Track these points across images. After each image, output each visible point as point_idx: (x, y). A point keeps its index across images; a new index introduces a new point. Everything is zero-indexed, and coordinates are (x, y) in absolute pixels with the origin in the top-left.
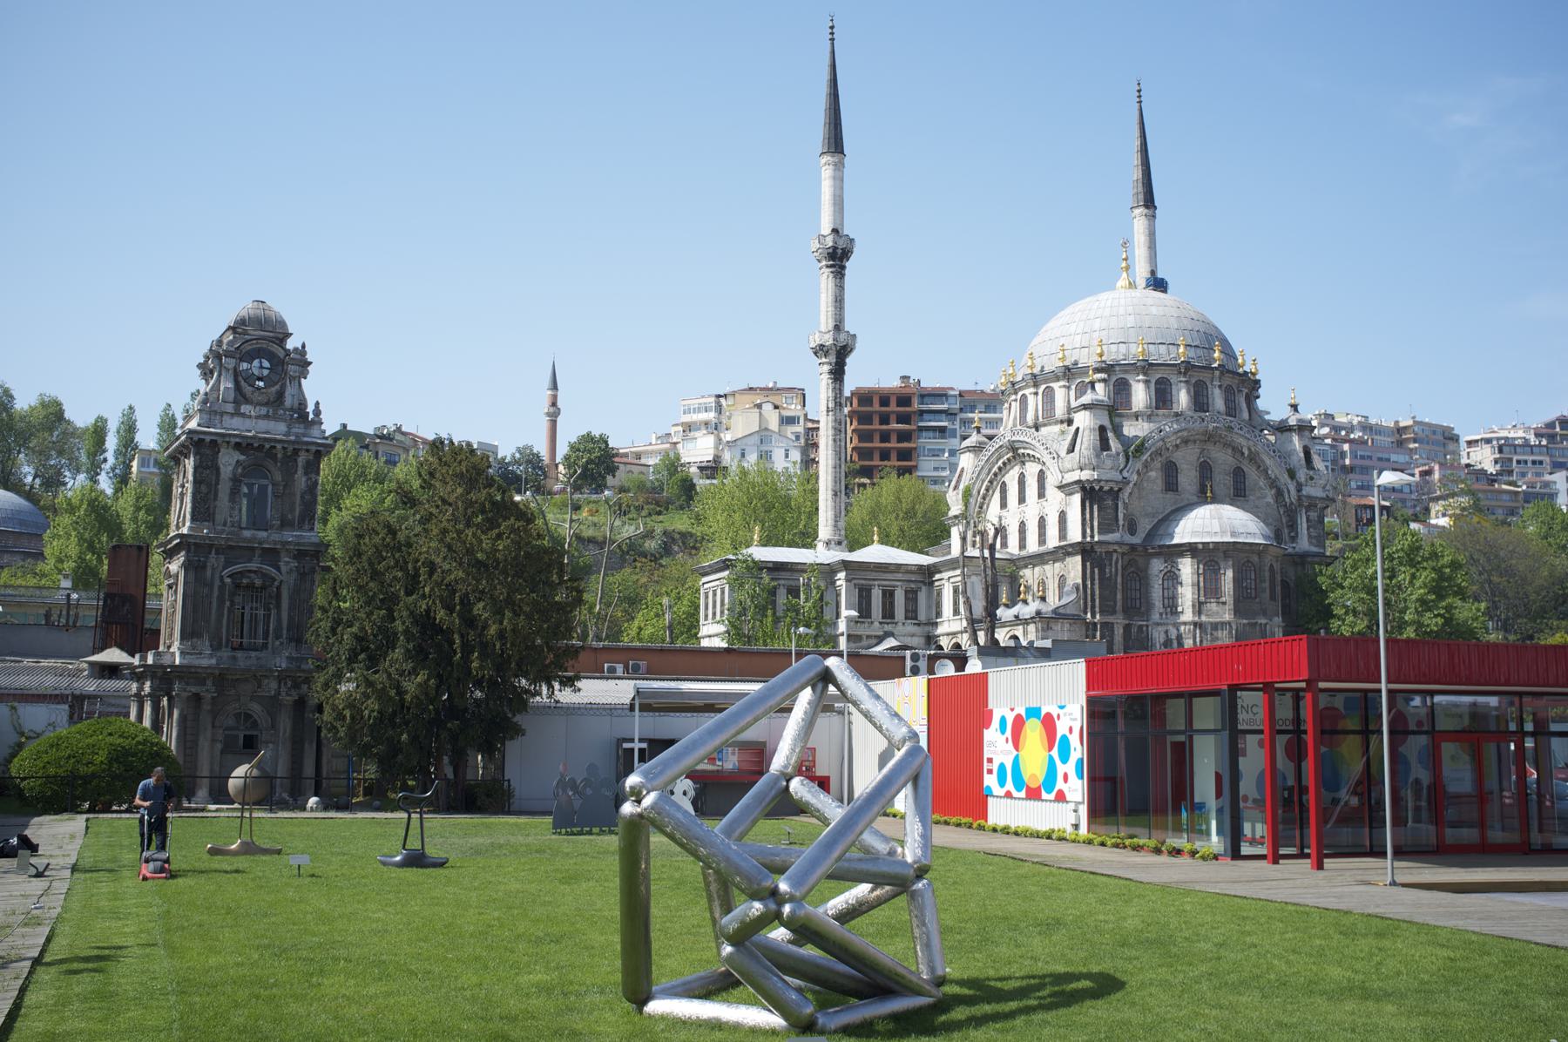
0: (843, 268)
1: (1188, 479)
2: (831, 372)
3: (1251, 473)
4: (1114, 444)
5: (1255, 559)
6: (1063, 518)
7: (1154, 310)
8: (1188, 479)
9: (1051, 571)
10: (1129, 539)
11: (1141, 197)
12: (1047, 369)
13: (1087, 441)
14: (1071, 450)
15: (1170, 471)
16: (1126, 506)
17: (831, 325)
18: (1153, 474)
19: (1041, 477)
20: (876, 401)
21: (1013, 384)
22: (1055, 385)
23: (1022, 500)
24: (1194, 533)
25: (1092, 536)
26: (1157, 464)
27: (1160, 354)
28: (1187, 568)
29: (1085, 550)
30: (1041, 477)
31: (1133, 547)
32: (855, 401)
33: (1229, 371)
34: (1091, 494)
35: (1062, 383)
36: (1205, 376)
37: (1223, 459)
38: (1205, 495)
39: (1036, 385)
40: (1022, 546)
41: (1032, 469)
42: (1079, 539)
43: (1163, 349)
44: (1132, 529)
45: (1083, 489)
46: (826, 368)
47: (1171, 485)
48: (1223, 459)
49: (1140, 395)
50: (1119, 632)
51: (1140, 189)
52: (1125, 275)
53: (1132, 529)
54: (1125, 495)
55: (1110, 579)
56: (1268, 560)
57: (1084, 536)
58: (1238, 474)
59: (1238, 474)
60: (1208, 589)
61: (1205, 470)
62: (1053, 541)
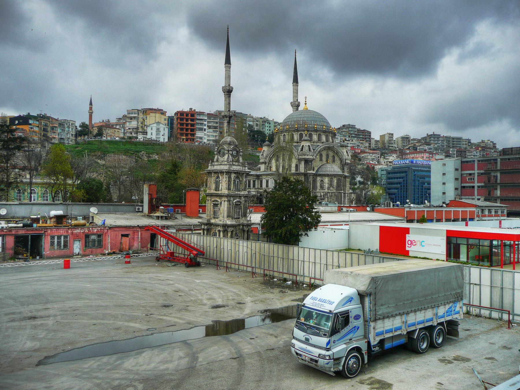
15: (321, 156)
20: (185, 115)
32: (179, 114)
59: (334, 157)
61: (328, 156)
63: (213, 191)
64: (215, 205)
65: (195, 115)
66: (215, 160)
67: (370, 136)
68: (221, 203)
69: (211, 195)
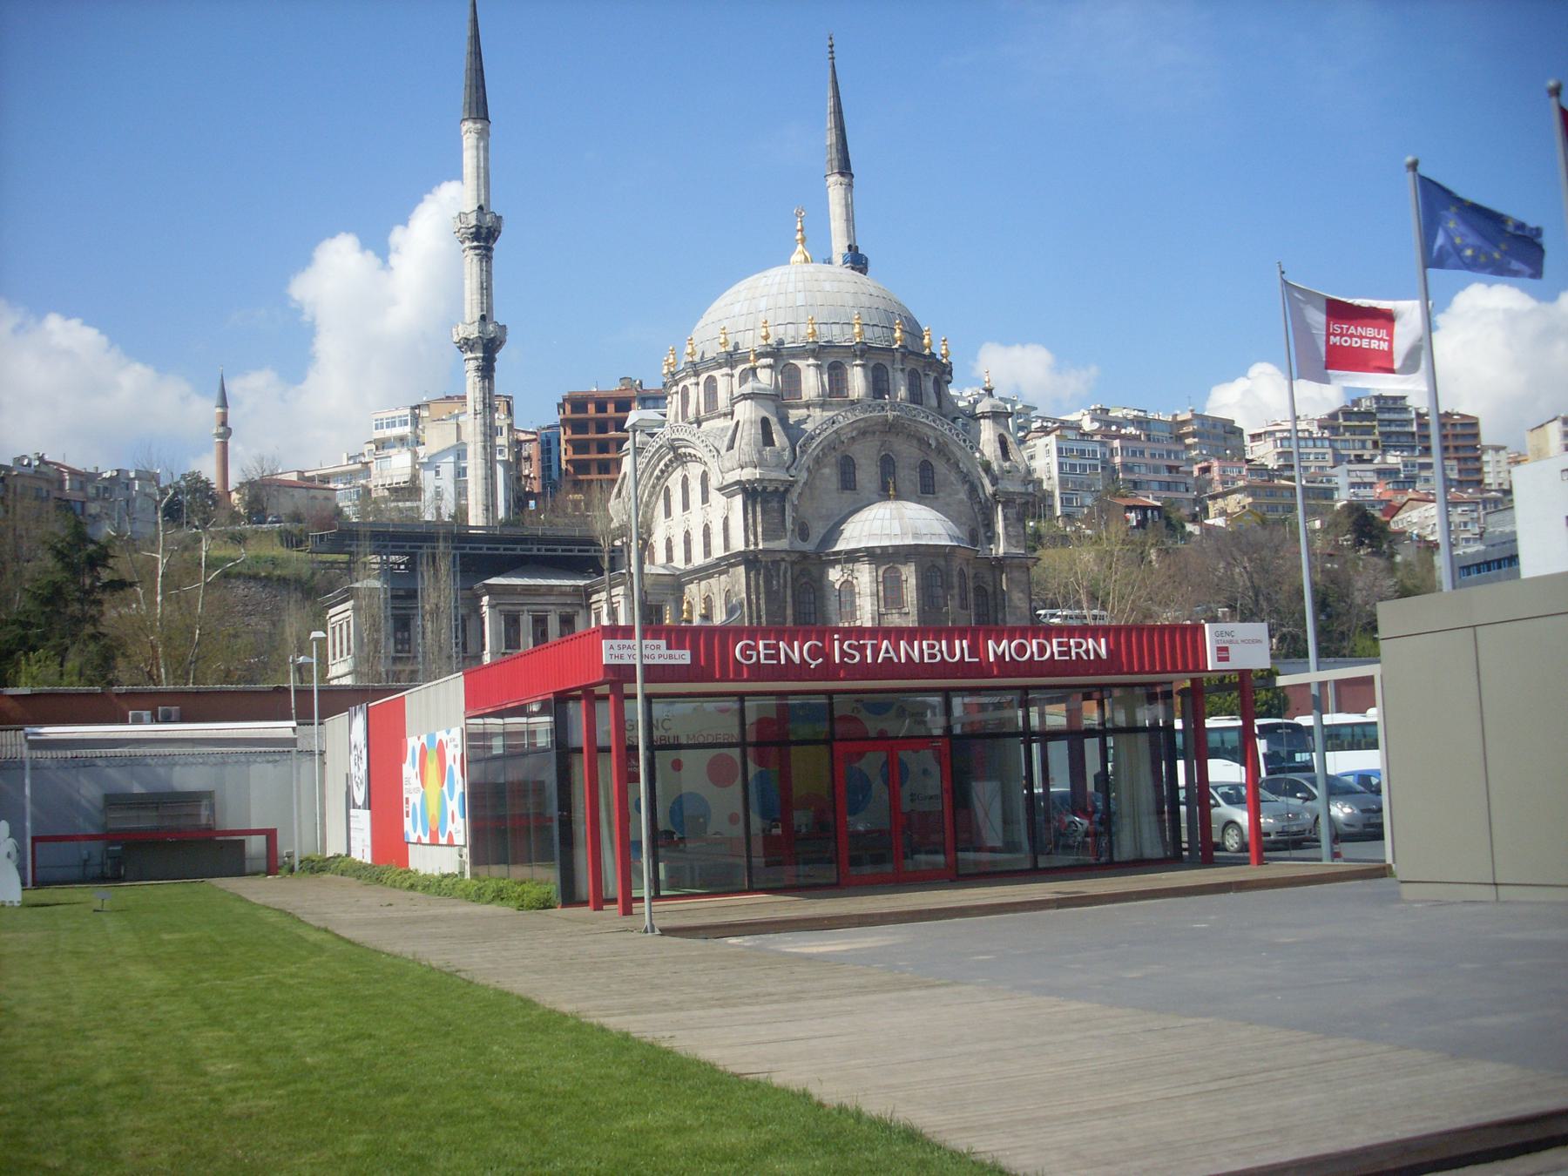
0: (489, 249)
1: (867, 475)
2: (478, 369)
3: (940, 467)
4: (779, 437)
5: (941, 563)
7: (827, 286)
8: (867, 475)
9: (718, 585)
10: (801, 546)
11: (835, 163)
12: (708, 356)
13: (749, 436)
14: (730, 447)
16: (795, 508)
17: (477, 316)
18: (827, 471)
19: (705, 478)
20: (591, 407)
21: (673, 375)
22: (716, 373)
23: (686, 506)
25: (756, 544)
26: (832, 458)
27: (838, 335)
28: (864, 577)
29: (749, 560)
30: (705, 478)
31: (804, 555)
32: (568, 407)
33: (912, 353)
34: (752, 493)
35: (726, 370)
36: (884, 360)
37: (907, 453)
38: (887, 491)
39: (697, 374)
40: (688, 559)
41: (695, 470)
42: (742, 548)
43: (836, 329)
44: (803, 533)
45: (745, 491)
46: (472, 365)
47: (848, 480)
48: (907, 453)
49: (811, 381)
51: (834, 155)
52: (800, 247)
53: (803, 533)
54: (793, 496)
55: (777, 592)
56: (956, 564)
57: (747, 544)
58: (926, 469)
59: (926, 469)
61: (887, 465)
62: (718, 551)
67: (1476, 436)
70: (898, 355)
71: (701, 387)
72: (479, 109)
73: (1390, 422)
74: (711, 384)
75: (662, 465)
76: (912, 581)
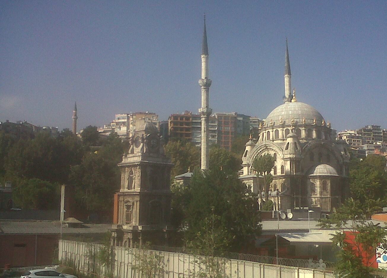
2: (205, 120)
6: (282, 167)
7: (306, 109)
14: (287, 148)
20: (179, 119)
24: (320, 173)
25: (293, 173)
35: (281, 129)
43: (309, 120)
44: (302, 171)
47: (312, 159)
50: (300, 200)
53: (302, 171)
60: (324, 187)
63: (126, 190)
64: (128, 207)
65: (191, 119)
66: (130, 152)
68: (133, 204)
69: (124, 195)
70: (323, 128)
71: (274, 132)
72: (206, 52)
73: (376, 133)
74: (277, 132)
75: (261, 150)
76: (329, 184)
